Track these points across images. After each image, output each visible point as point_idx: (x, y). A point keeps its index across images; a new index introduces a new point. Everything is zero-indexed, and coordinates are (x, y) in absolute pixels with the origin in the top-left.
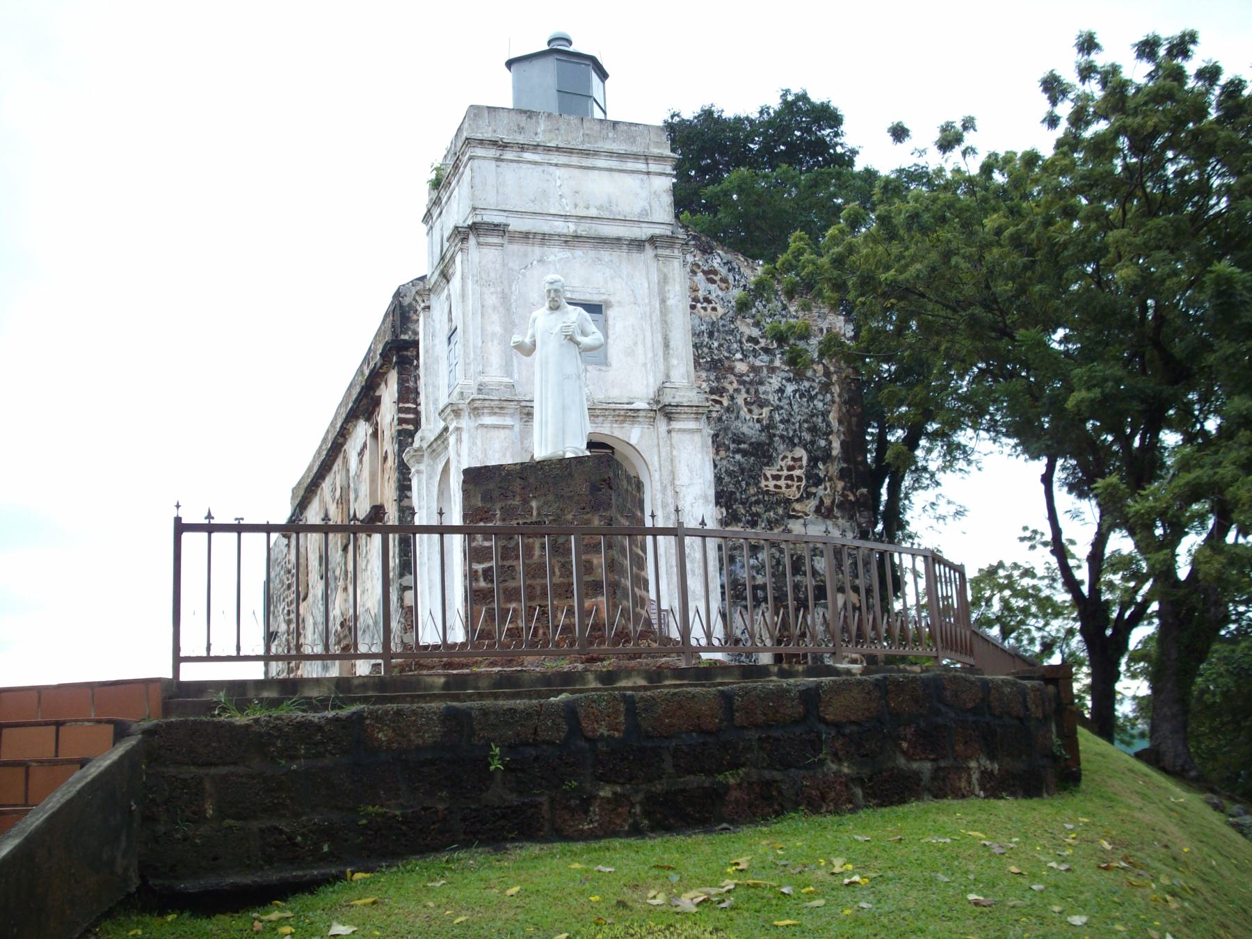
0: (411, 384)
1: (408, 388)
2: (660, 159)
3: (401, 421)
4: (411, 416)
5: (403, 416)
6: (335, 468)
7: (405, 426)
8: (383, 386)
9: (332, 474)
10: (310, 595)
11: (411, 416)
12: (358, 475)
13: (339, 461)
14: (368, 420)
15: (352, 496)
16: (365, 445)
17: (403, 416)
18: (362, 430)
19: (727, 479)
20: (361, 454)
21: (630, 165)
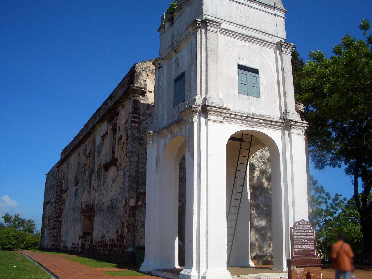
0: (138, 106)
1: (137, 107)
2: (280, 10)
3: (133, 122)
4: (138, 120)
5: (134, 120)
6: (87, 142)
7: (134, 124)
8: (120, 107)
9: (84, 145)
10: (68, 191)
11: (138, 120)
12: (101, 146)
13: (90, 140)
14: (109, 122)
15: (96, 154)
16: (106, 133)
17: (134, 120)
18: (104, 127)
19: (260, 160)
20: (103, 137)
21: (268, 10)
